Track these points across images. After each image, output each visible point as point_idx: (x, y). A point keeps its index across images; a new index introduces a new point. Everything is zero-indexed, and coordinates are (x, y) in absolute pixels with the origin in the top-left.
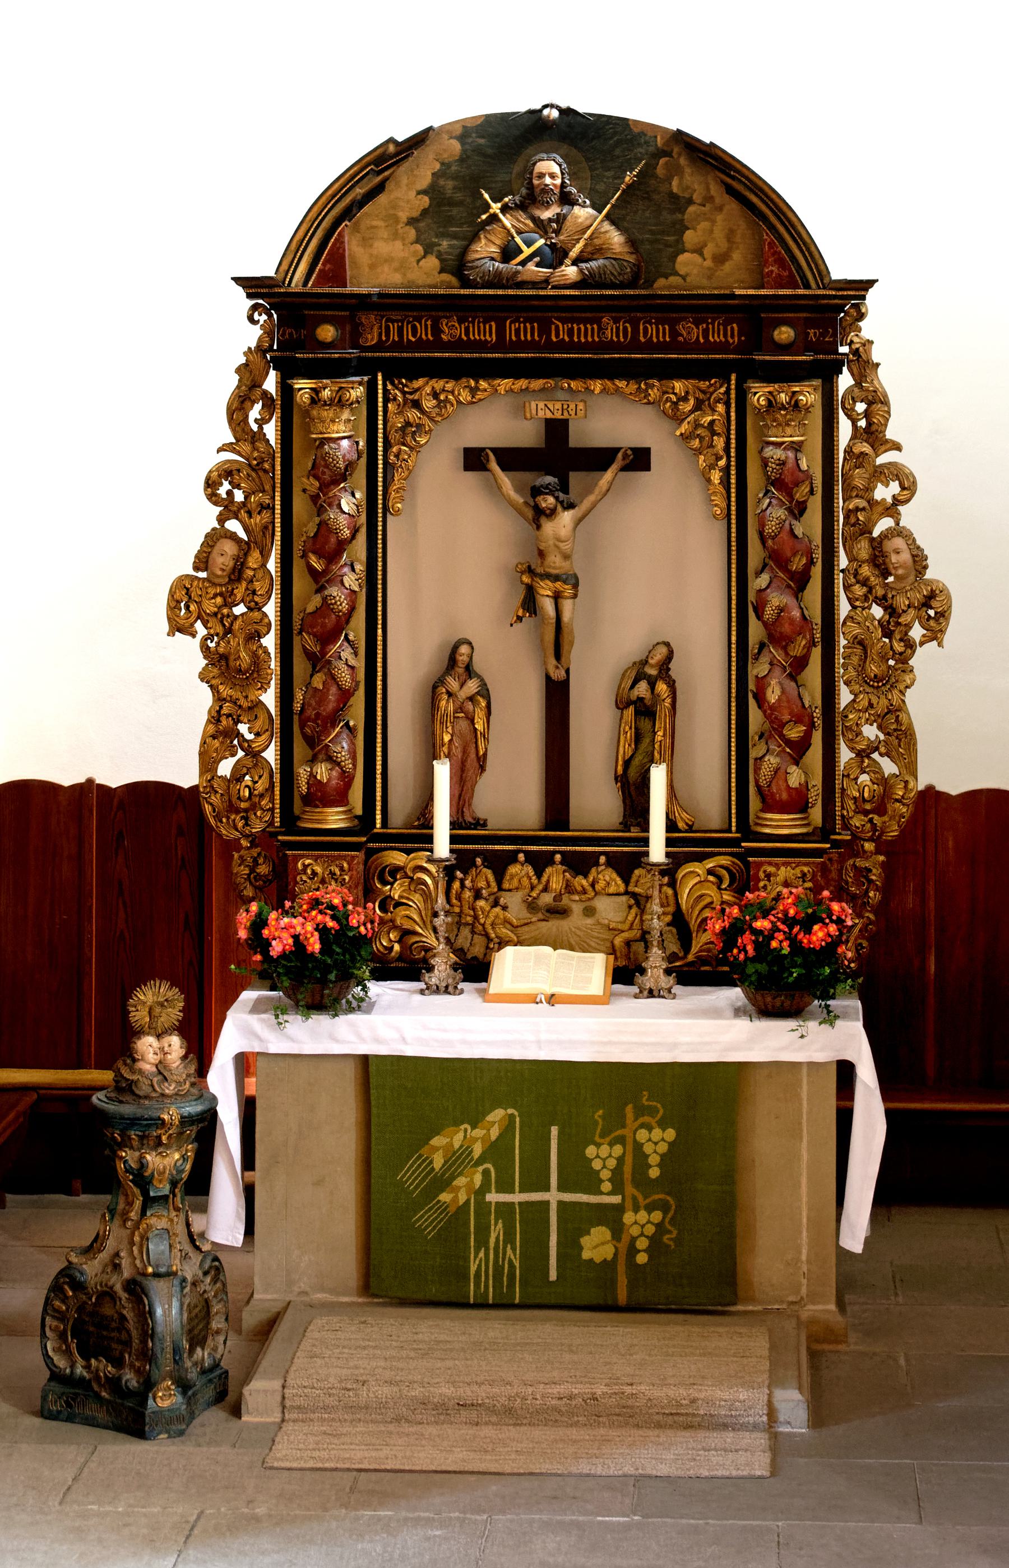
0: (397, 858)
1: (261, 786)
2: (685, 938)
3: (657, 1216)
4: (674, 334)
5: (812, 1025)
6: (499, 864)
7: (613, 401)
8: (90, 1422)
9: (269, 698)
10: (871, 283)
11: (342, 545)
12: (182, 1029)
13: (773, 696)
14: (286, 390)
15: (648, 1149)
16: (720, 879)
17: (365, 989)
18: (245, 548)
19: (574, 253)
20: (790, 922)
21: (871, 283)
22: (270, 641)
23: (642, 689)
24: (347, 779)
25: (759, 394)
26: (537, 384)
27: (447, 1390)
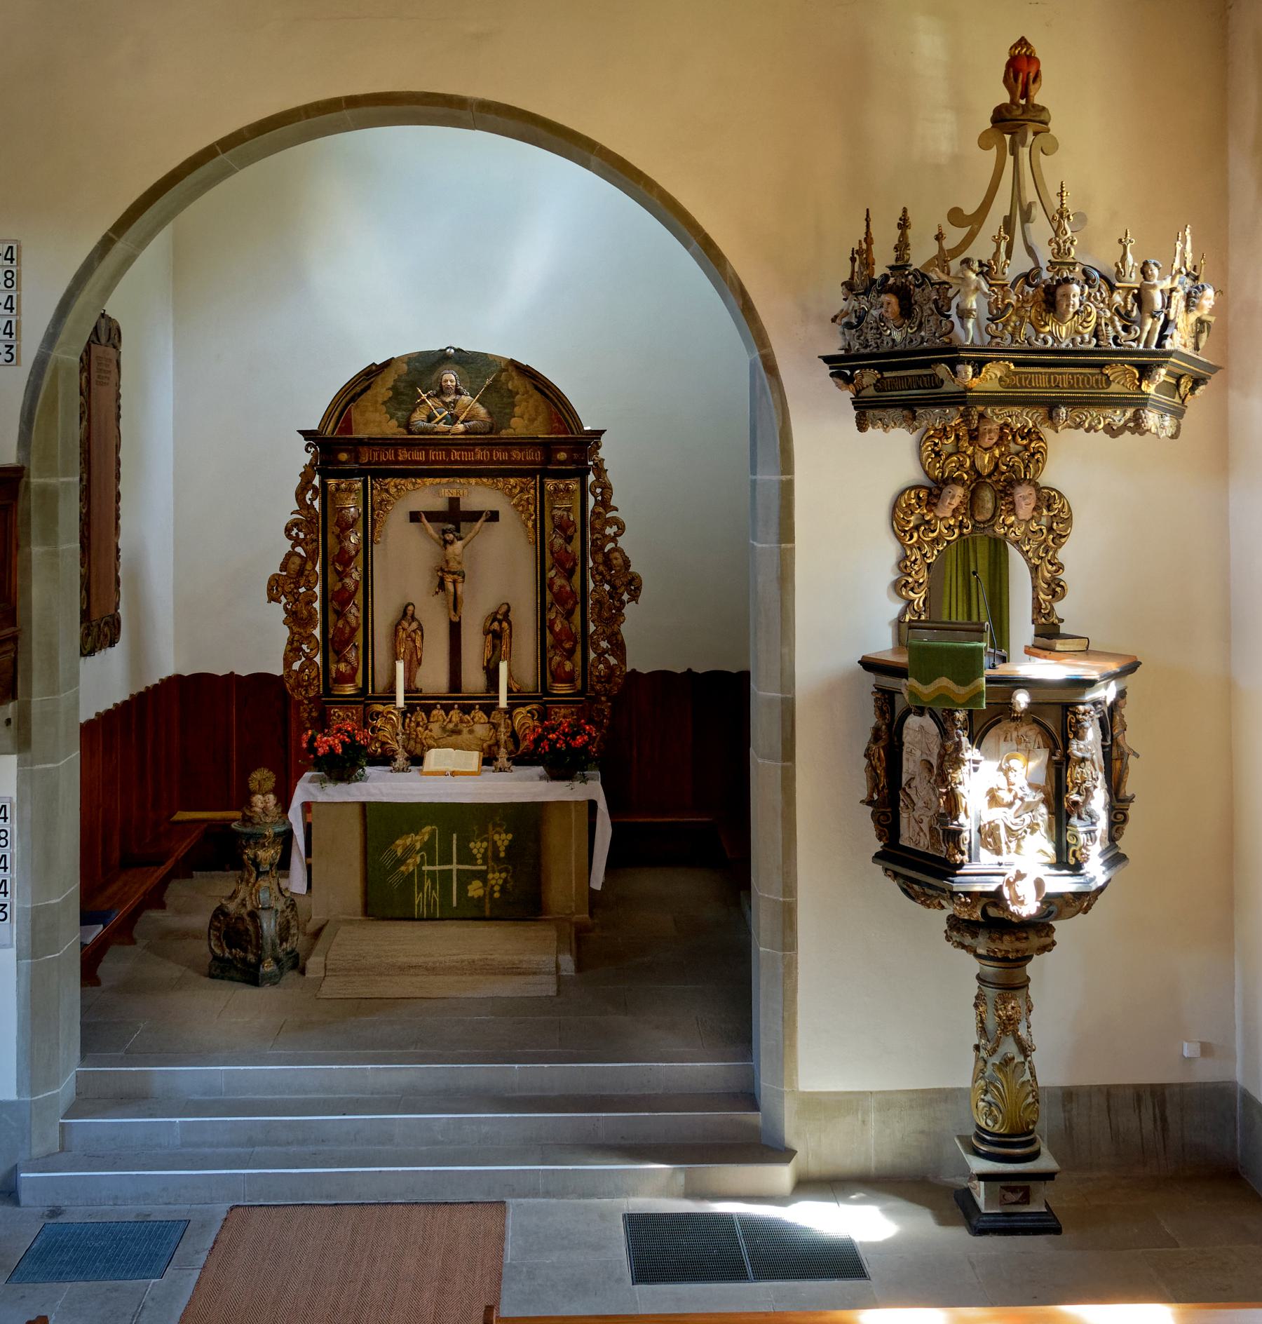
0: (379, 708)
1: (314, 674)
2: (517, 744)
3: (504, 875)
4: (510, 456)
5: (577, 783)
6: (428, 710)
7: (480, 489)
8: (232, 979)
9: (317, 632)
10: (603, 432)
11: (351, 559)
12: (275, 791)
13: (558, 627)
14: (323, 484)
15: (499, 843)
16: (533, 716)
17: (363, 770)
18: (304, 561)
19: (462, 418)
20: (565, 734)
21: (603, 432)
22: (317, 605)
23: (496, 625)
24: (355, 670)
25: (550, 484)
26: (445, 480)
27: (405, 959)
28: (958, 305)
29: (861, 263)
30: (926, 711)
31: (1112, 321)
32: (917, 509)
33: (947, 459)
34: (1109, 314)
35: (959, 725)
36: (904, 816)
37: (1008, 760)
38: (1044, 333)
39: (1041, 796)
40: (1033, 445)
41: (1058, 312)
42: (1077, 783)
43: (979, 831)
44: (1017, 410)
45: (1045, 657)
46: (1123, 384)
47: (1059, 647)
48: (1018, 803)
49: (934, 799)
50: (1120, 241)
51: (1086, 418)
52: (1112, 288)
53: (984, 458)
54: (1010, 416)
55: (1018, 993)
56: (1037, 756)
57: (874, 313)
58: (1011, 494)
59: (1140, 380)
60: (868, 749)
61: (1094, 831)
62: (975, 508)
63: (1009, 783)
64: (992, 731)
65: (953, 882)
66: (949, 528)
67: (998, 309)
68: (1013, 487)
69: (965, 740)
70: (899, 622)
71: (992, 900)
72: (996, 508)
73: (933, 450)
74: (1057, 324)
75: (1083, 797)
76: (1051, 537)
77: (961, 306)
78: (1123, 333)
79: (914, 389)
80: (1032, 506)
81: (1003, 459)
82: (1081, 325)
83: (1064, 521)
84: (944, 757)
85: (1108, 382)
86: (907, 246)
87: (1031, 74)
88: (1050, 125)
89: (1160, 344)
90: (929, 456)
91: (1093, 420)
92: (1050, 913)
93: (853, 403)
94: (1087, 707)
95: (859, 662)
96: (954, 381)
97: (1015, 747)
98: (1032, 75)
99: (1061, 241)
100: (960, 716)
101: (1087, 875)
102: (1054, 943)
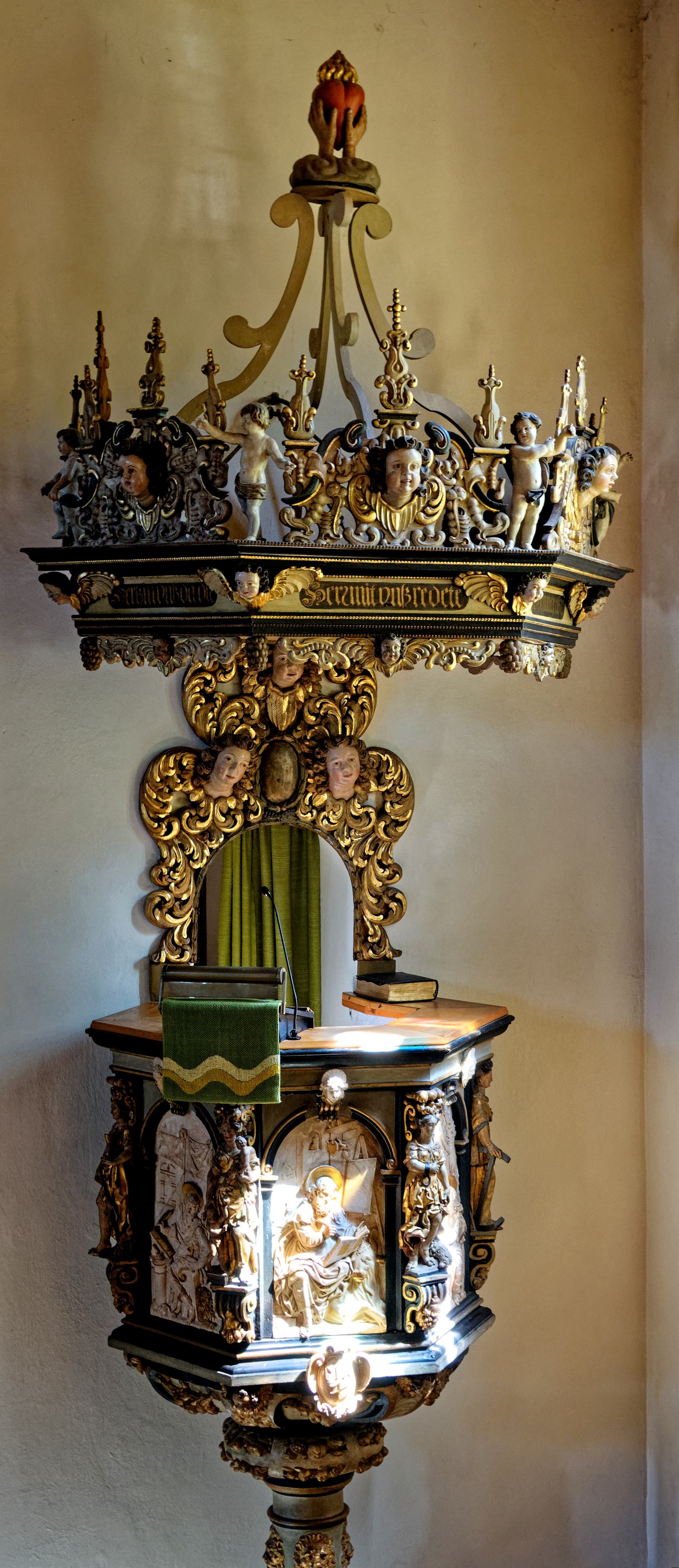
28: (238, 479)
29: (89, 402)
30: (191, 1106)
31: (468, 503)
32: (177, 784)
33: (224, 705)
34: (464, 495)
35: (241, 1128)
36: (158, 1270)
37: (315, 1179)
38: (368, 523)
39: (365, 1230)
40: (355, 683)
41: (389, 491)
42: (417, 1209)
43: (272, 1290)
44: (327, 641)
45: (373, 1011)
46: (485, 602)
47: (393, 996)
48: (330, 1242)
49: (202, 1242)
50: (481, 383)
51: (431, 653)
52: (469, 456)
53: (281, 704)
54: (316, 652)
55: (330, 1533)
56: (360, 1171)
57: (110, 483)
58: (323, 760)
59: (510, 596)
60: (102, 1167)
61: (442, 1281)
62: (269, 780)
63: (317, 1214)
64: (292, 1135)
65: (231, 1372)
66: (228, 814)
67: (299, 485)
68: (326, 750)
69: (249, 1150)
70: (151, 961)
71: (289, 1396)
72: (299, 781)
73: (202, 692)
74: (387, 508)
75: (427, 1230)
76: (382, 824)
77: (244, 479)
78: (485, 525)
79: (170, 605)
80: (354, 777)
81: (311, 705)
82: (423, 511)
83: (401, 799)
84: (218, 1178)
86: (160, 379)
87: (351, 111)
88: (380, 193)
89: (539, 541)
90: (196, 702)
91: (441, 656)
92: (378, 1409)
93: (77, 624)
94: (433, 1093)
95: (87, 1031)
96: (230, 594)
97: (326, 1157)
98: (352, 113)
99: (393, 382)
100: (243, 1113)
101: (431, 1348)
102: (384, 1452)
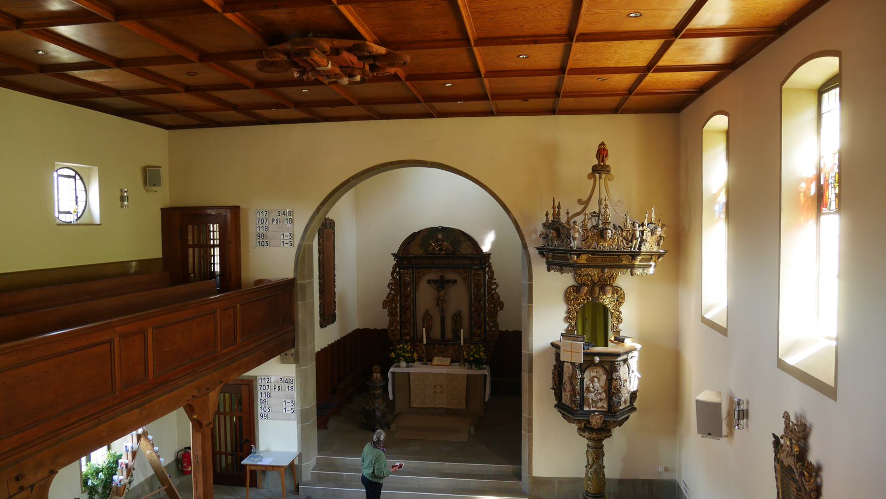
0: (418, 344)
9: (398, 319)
22: (398, 310)
58: (604, 289)
78: (626, 245)
85: (622, 261)
88: (611, 172)
98: (605, 155)
102: (611, 435)
